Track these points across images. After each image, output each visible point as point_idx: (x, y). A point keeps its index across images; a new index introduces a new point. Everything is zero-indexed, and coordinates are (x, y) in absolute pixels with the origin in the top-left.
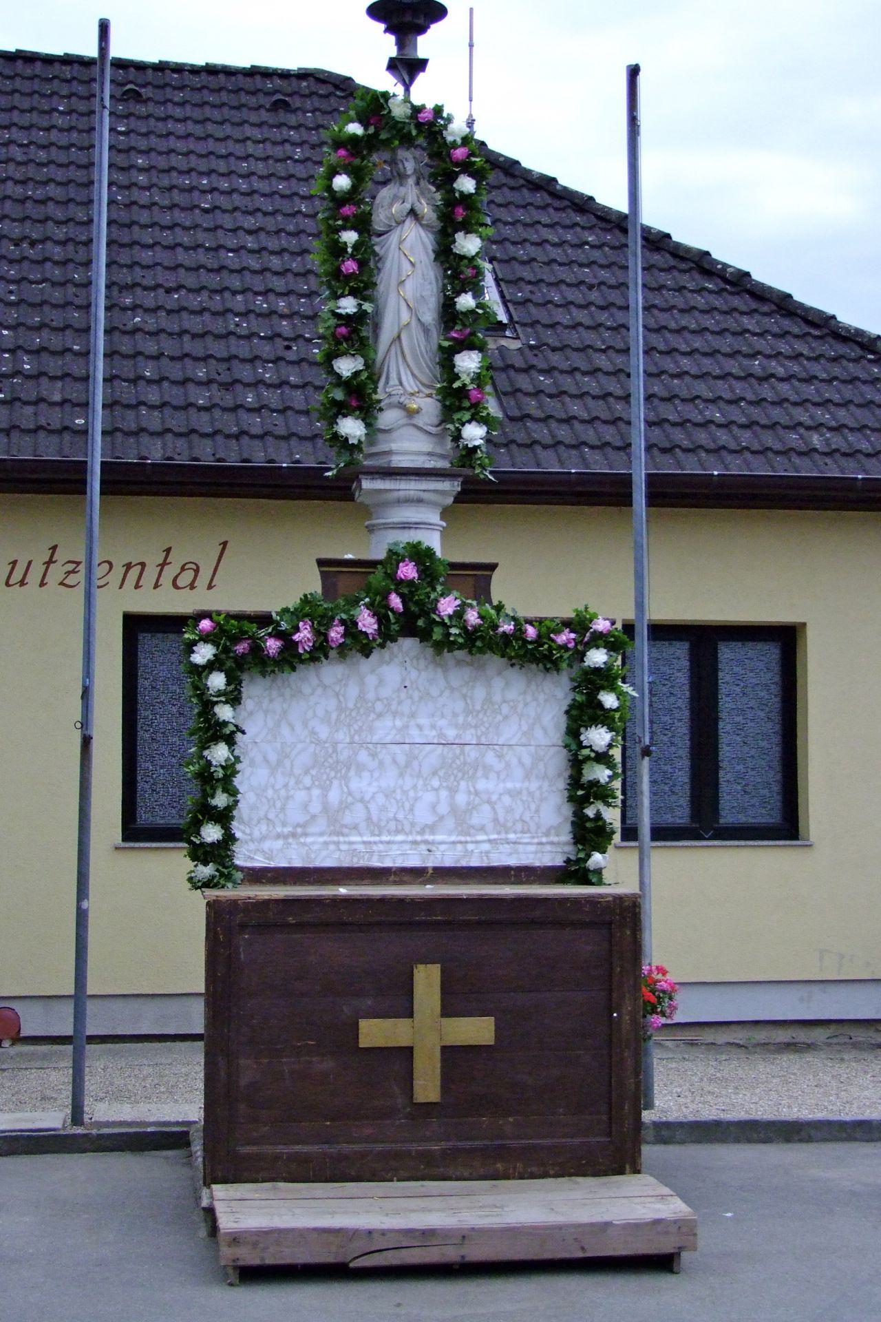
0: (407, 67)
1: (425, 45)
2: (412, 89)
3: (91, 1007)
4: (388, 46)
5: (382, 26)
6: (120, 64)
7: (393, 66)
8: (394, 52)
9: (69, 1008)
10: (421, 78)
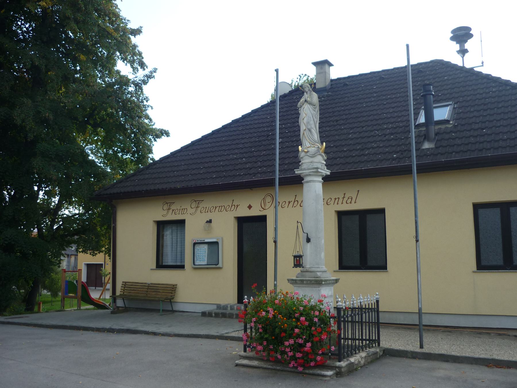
0: (463, 52)
1: (467, 46)
2: (464, 58)
3: (424, 316)
4: (457, 47)
5: (455, 42)
6: (412, 66)
7: (458, 52)
8: (458, 49)
9: (417, 316)
10: (467, 55)
